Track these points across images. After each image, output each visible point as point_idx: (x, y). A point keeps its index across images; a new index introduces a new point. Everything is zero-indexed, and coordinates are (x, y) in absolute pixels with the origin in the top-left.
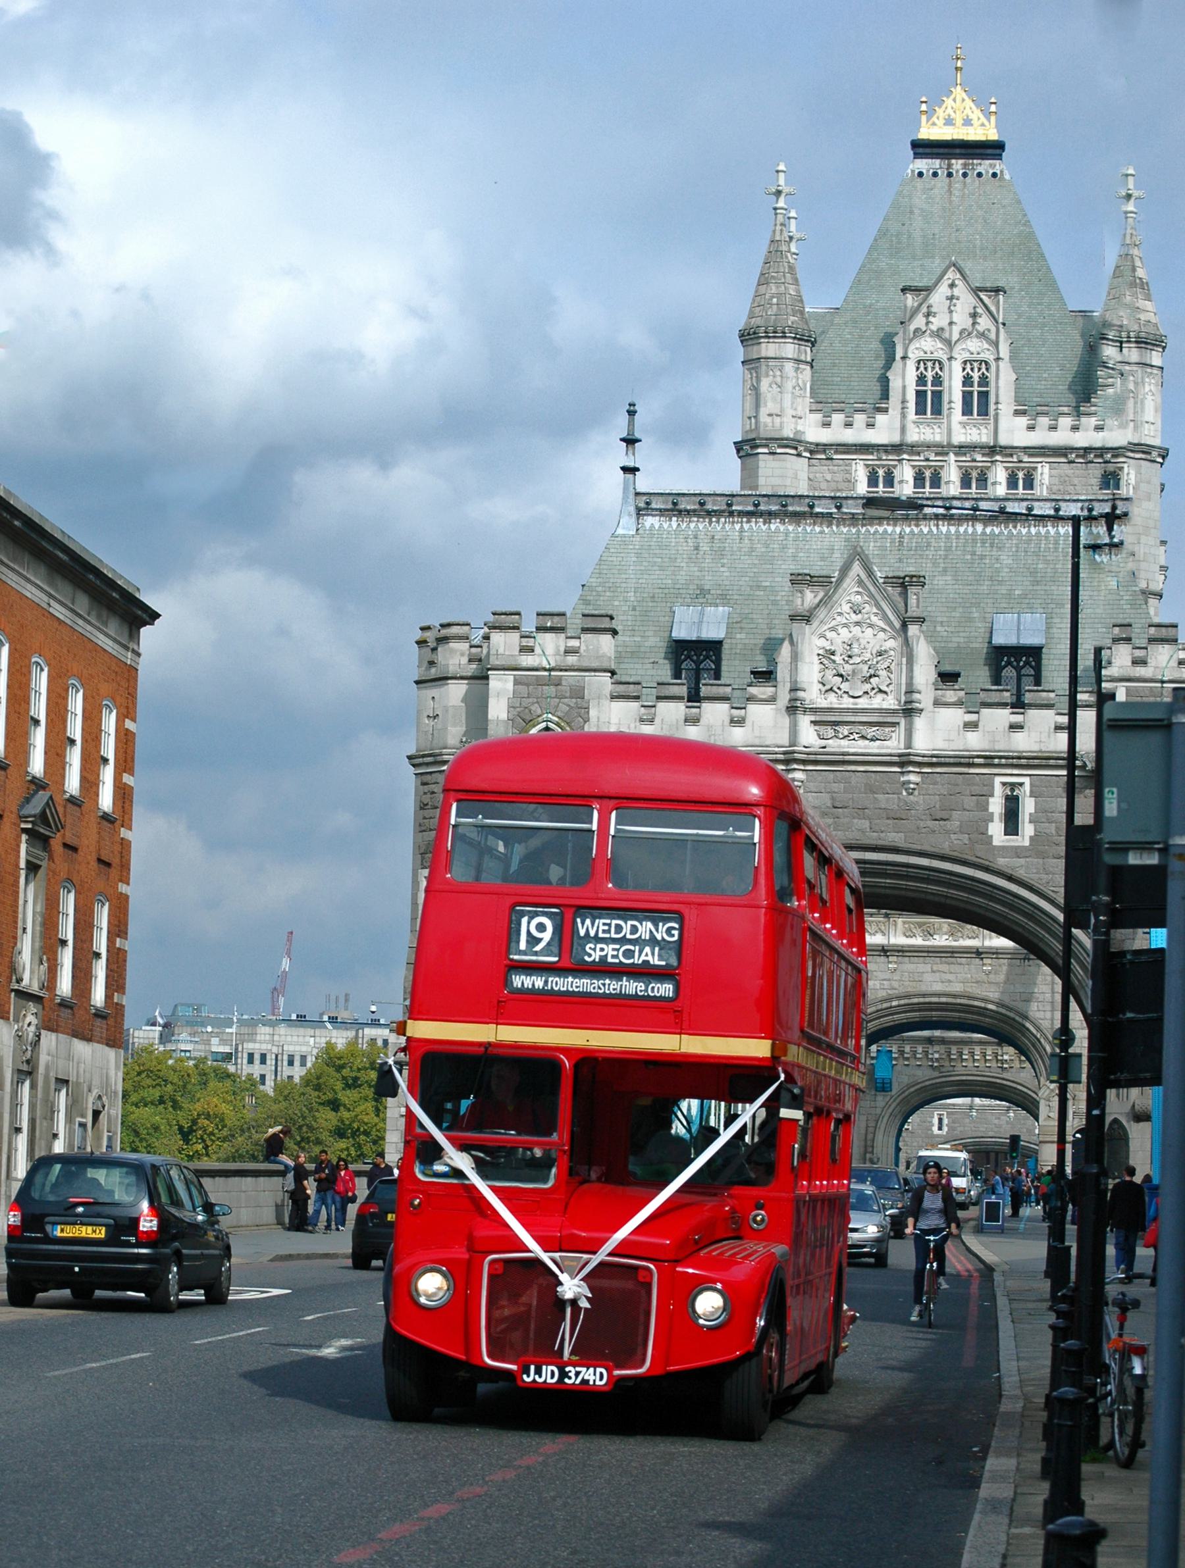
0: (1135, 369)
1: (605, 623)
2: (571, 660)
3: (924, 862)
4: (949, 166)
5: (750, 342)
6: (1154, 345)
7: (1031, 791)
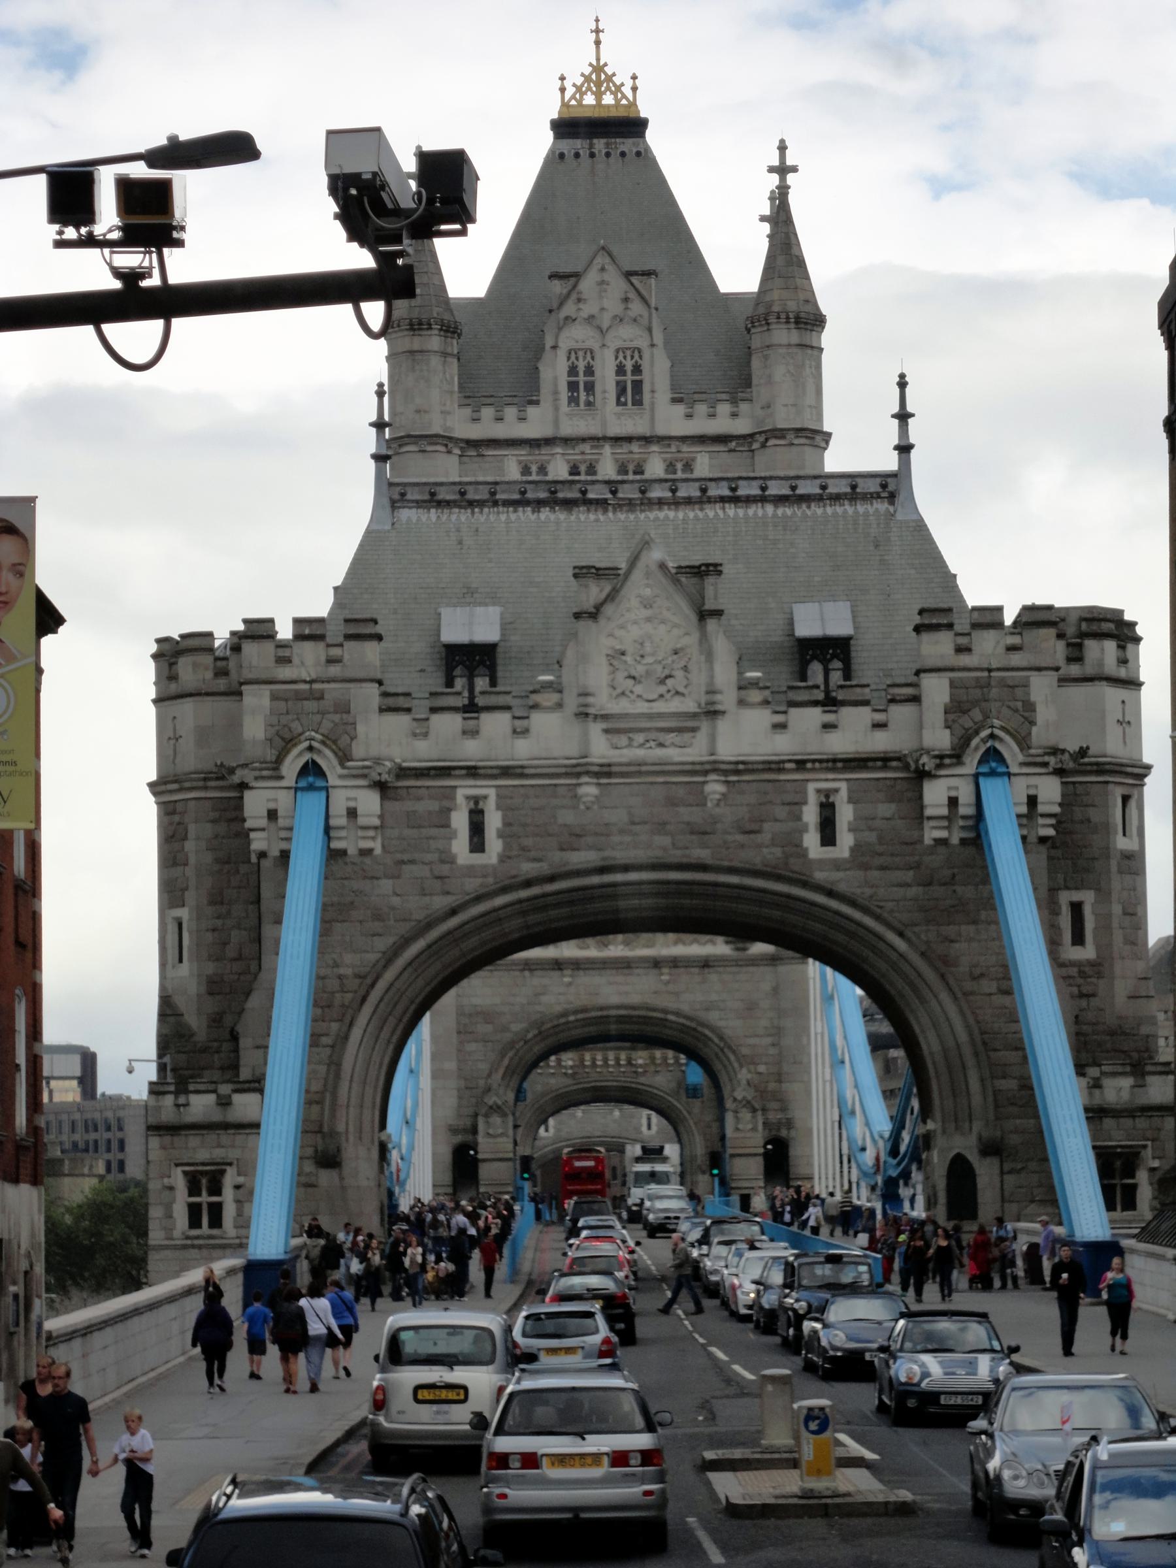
0: (795, 350)
1: (369, 629)
2: (334, 670)
3: (734, 879)
4: (591, 146)
6: (814, 325)
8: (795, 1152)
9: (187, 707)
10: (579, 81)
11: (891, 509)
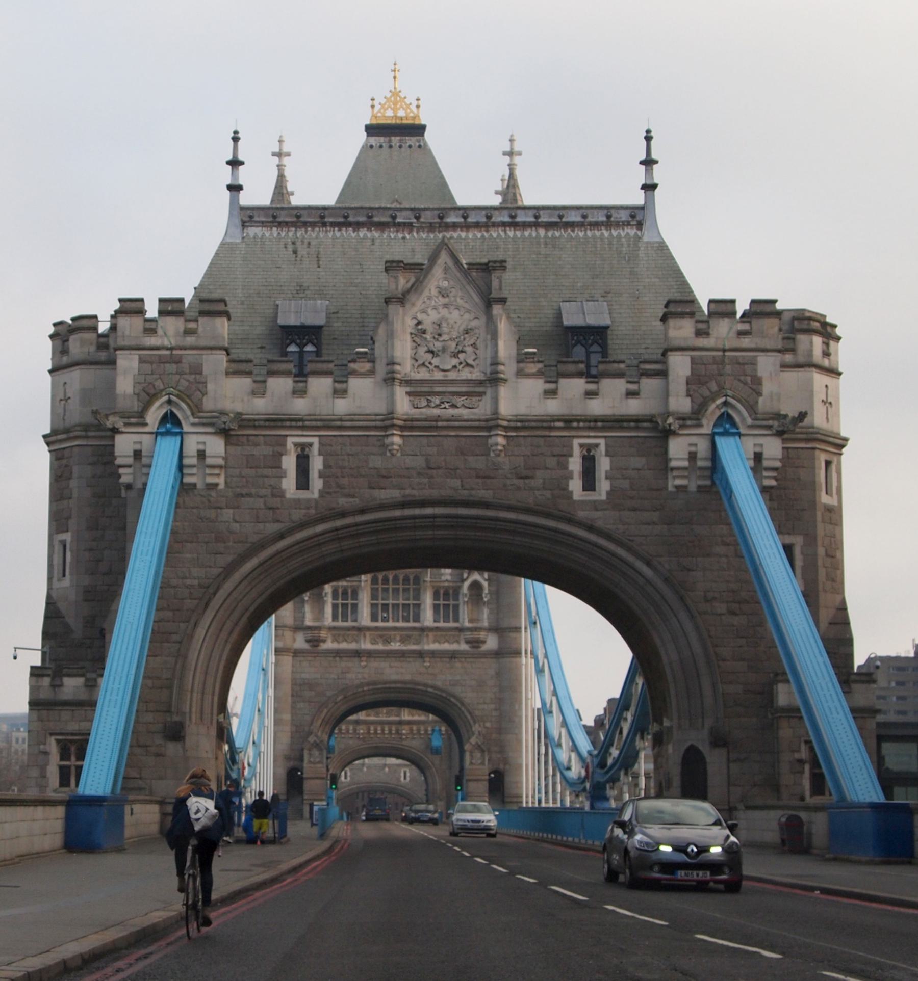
1: (221, 307)
2: (190, 340)
4: (390, 141)
7: (607, 451)
8: (507, 779)
9: (75, 376)
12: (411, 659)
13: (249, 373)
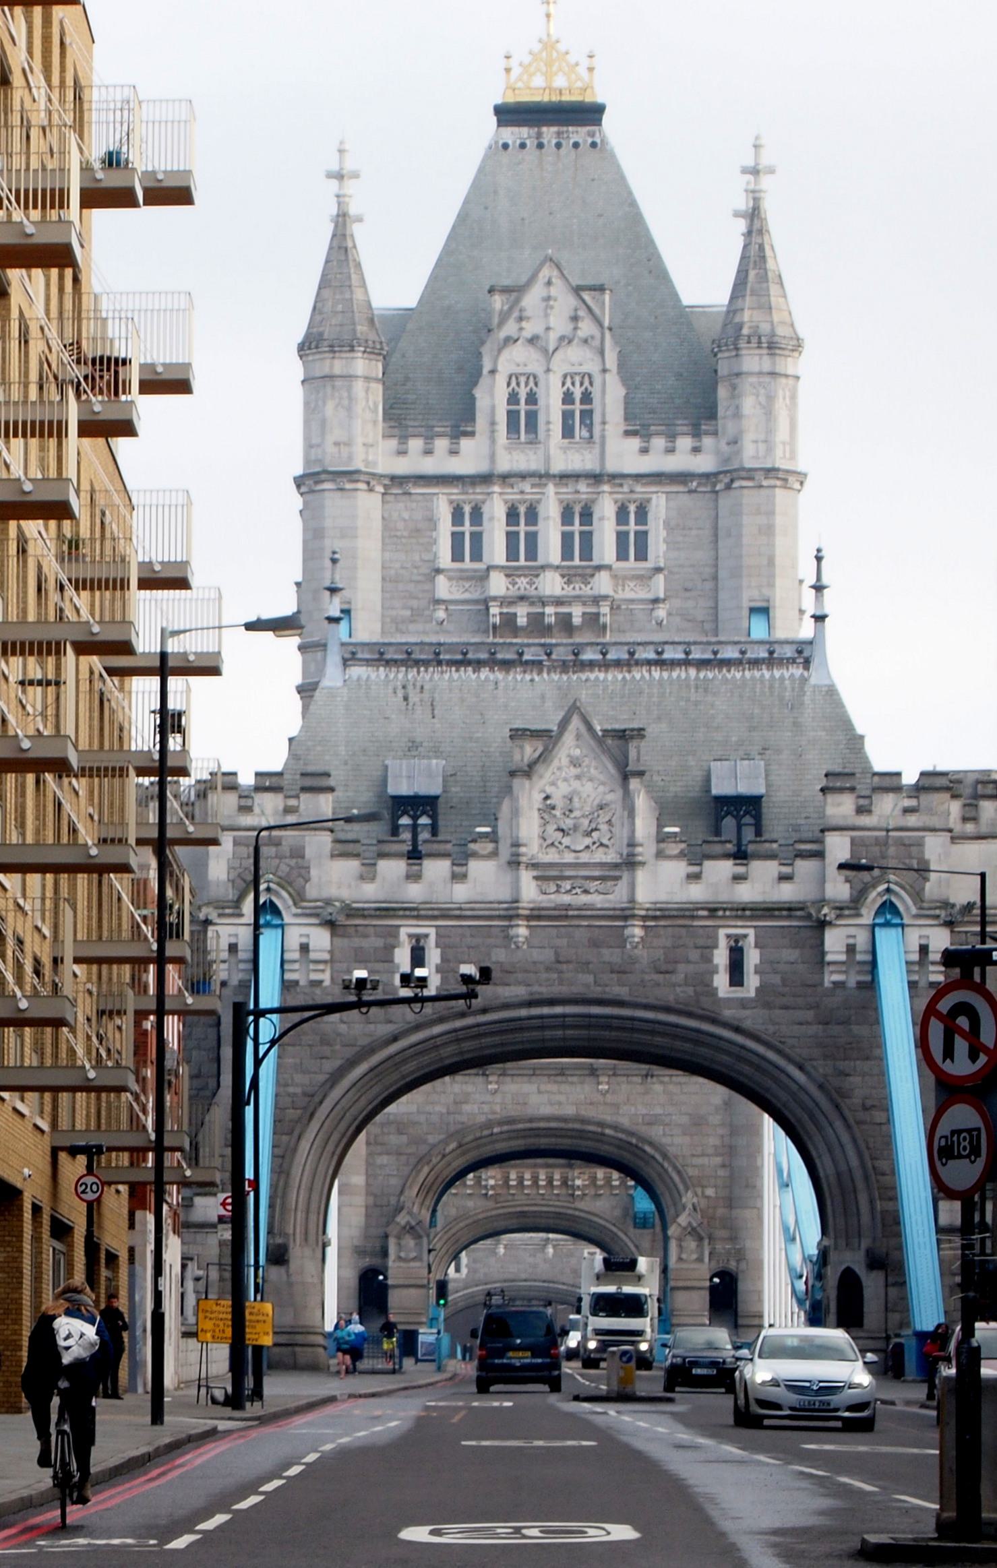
2: (291, 819)
3: (650, 1015)
4: (539, 135)
5: (310, 358)
8: (742, 1286)
10: (527, 59)
11: (806, 674)
12: (575, 1079)
13: (357, 855)
